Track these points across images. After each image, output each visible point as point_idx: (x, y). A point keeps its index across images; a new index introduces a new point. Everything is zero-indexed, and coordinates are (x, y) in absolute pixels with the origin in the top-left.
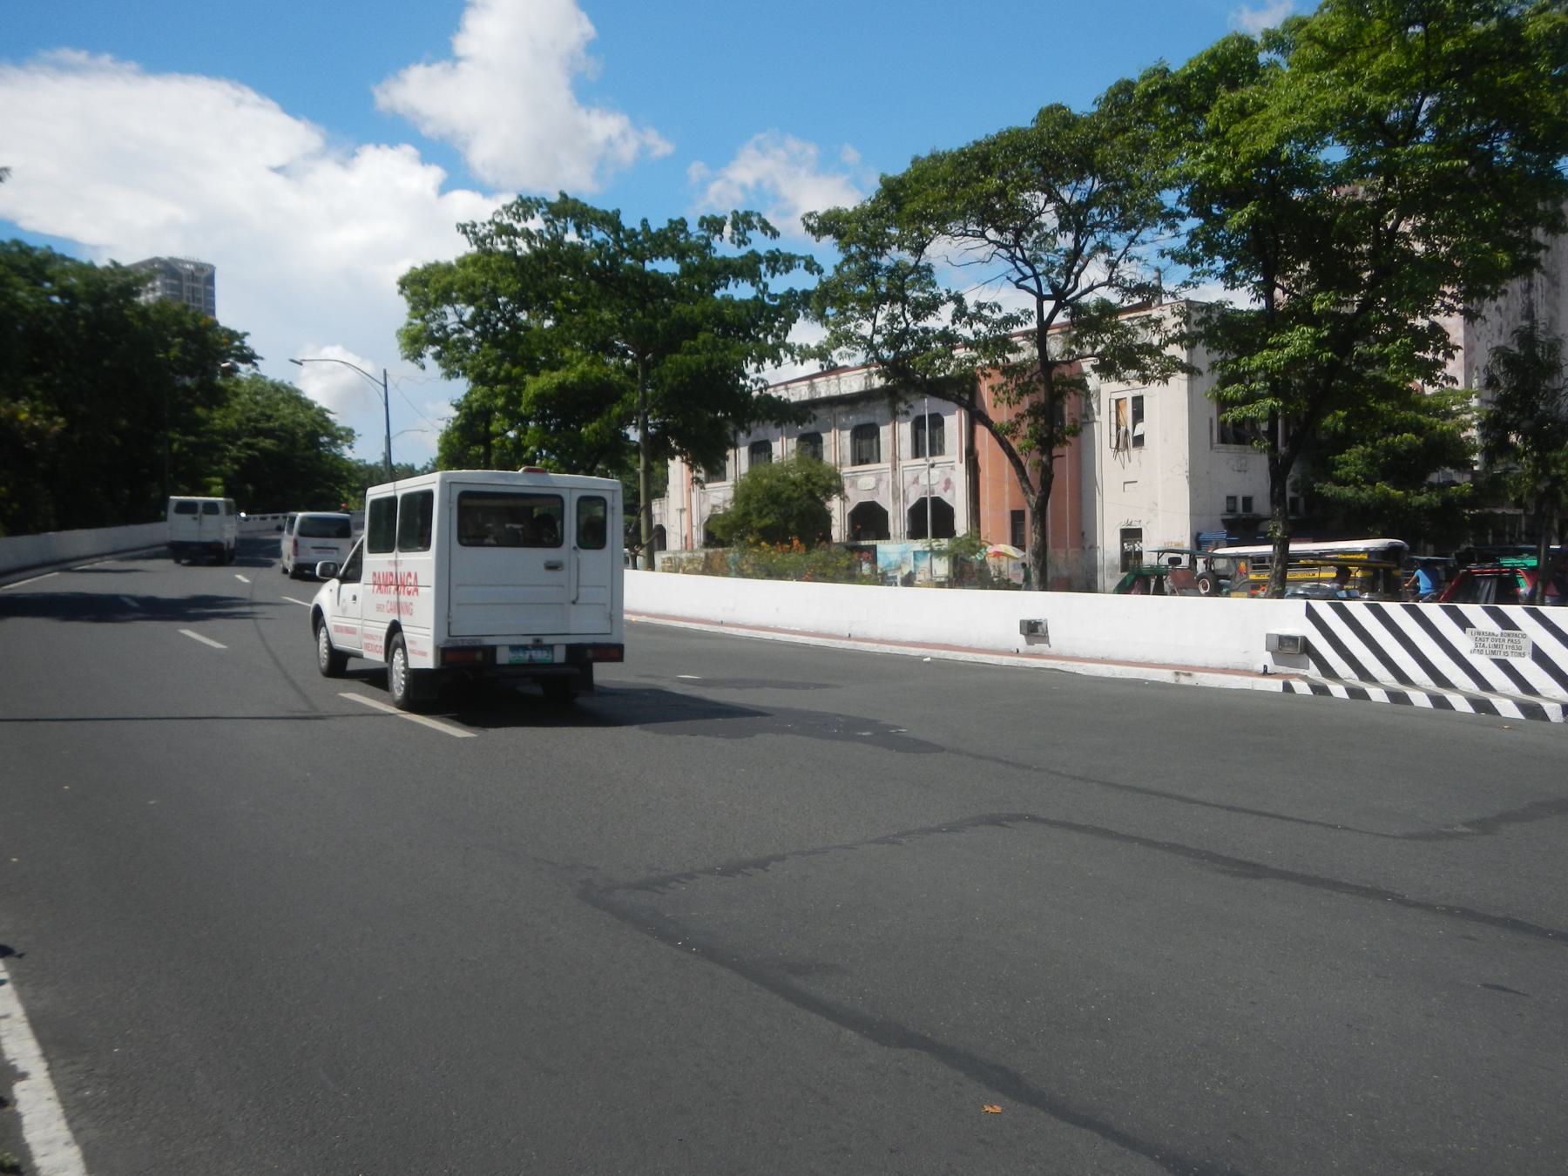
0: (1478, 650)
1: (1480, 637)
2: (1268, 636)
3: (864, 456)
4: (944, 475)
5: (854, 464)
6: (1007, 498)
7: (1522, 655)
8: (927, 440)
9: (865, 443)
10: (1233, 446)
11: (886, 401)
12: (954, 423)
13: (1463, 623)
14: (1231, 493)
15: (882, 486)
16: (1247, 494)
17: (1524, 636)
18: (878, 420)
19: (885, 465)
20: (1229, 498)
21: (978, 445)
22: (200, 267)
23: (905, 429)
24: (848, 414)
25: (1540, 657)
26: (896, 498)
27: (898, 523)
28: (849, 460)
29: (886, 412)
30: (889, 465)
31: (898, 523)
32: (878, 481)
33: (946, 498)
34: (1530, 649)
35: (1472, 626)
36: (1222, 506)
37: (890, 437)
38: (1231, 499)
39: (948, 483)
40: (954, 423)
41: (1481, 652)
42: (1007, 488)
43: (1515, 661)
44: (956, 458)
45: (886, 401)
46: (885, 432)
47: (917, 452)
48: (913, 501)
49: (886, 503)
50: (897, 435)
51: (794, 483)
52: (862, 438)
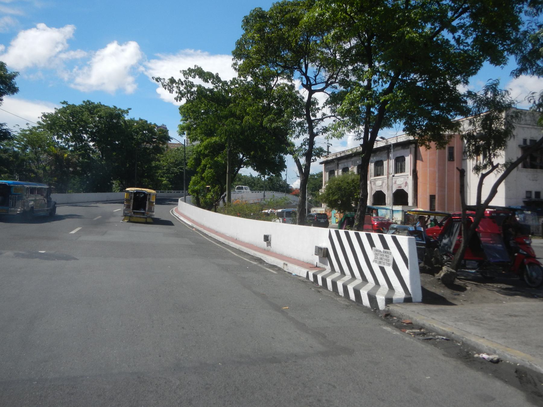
0: (375, 261)
1: (377, 252)
2: (316, 247)
3: (379, 173)
4: (404, 181)
5: (375, 176)
6: (428, 190)
7: (389, 265)
8: (399, 167)
9: (379, 168)
10: (529, 170)
11: (386, 151)
12: (409, 160)
13: (372, 245)
14: (529, 189)
15: (384, 184)
16: (538, 189)
17: (391, 253)
18: (383, 159)
19: (385, 176)
20: (527, 192)
21: (418, 168)
22: (181, 113)
23: (392, 162)
24: (373, 157)
25: (395, 268)
26: (388, 189)
27: (389, 199)
28: (373, 175)
29: (386, 155)
30: (386, 176)
31: (389, 199)
32: (383, 183)
33: (405, 190)
34: (391, 262)
35: (375, 246)
36: (523, 195)
37: (387, 166)
38: (529, 193)
39: (406, 183)
40: (409, 160)
42: (428, 186)
44: (409, 173)
45: (386, 151)
46: (385, 163)
47: (396, 172)
48: (394, 191)
49: (385, 192)
50: (389, 165)
51: (348, 183)
52: (378, 166)
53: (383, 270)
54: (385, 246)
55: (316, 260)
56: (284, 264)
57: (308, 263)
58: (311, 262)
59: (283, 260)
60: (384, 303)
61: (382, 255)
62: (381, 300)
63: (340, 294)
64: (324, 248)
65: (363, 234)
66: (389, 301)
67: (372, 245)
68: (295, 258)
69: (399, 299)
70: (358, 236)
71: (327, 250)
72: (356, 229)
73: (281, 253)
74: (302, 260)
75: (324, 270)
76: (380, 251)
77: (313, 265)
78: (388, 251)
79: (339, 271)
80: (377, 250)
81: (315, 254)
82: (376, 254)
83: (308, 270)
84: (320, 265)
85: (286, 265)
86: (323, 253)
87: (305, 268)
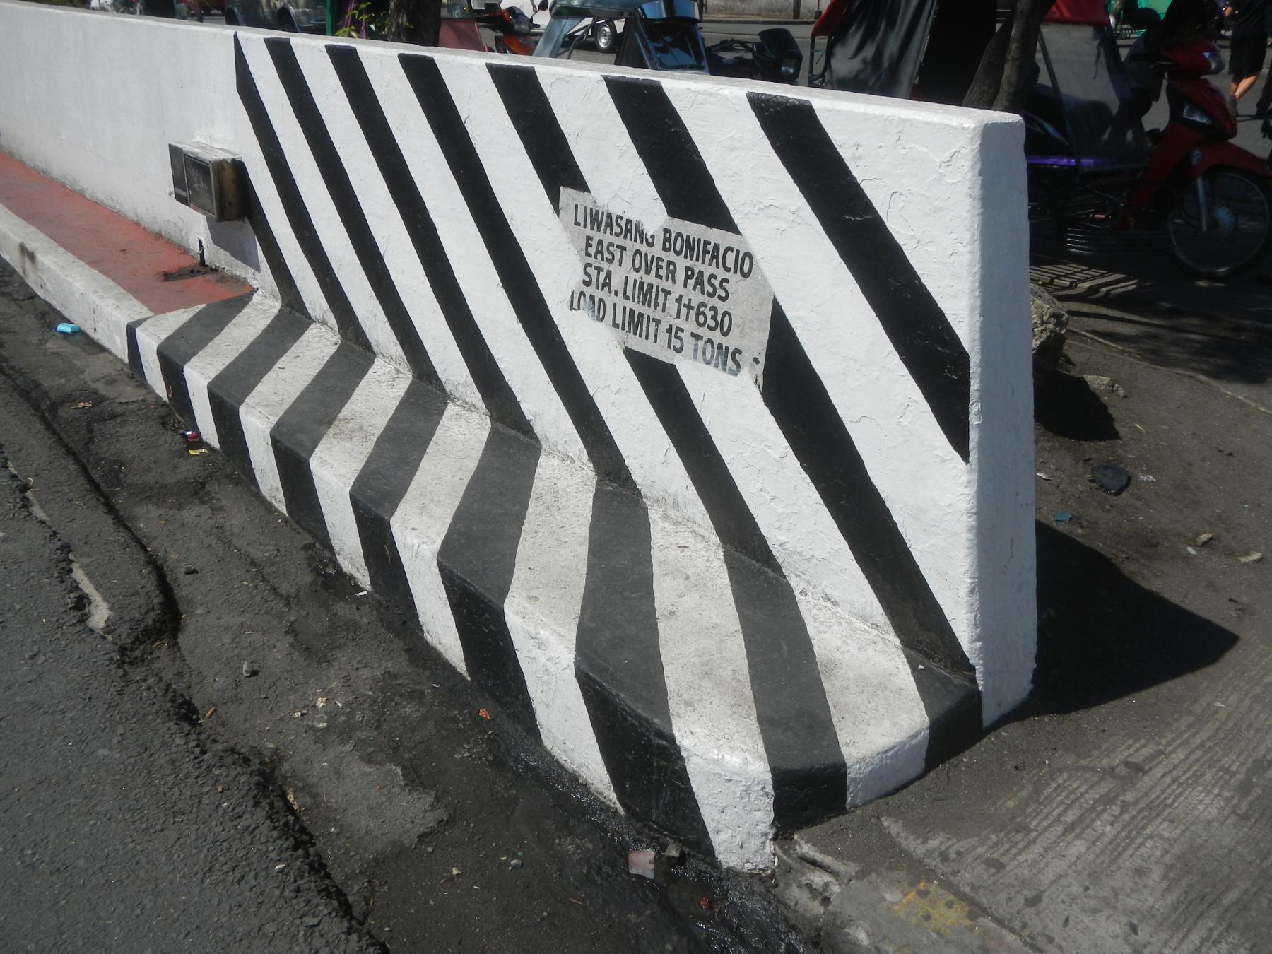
7: (728, 359)
13: (556, 165)
17: (745, 264)
34: (753, 340)
35: (579, 183)
41: (598, 309)
43: (703, 383)
53: (663, 387)
54: (687, 184)
55: (194, 228)
56: (23, 249)
57: (158, 236)
58: (175, 235)
59: (29, 214)
60: (764, 814)
61: (649, 264)
62: (725, 761)
63: (347, 567)
64: (220, 165)
65: (468, 74)
66: (808, 791)
67: (556, 165)
68: (101, 197)
69: (895, 754)
70: (427, 82)
71: (238, 168)
72: (403, 20)
73: (41, 165)
74: (131, 215)
75: (241, 298)
76: (633, 231)
77: (183, 250)
78: (715, 236)
79: (332, 320)
80: (597, 219)
81: (180, 198)
82: (595, 251)
83: (132, 309)
84: (218, 257)
85: (32, 256)
86: (222, 192)
87: (134, 288)
